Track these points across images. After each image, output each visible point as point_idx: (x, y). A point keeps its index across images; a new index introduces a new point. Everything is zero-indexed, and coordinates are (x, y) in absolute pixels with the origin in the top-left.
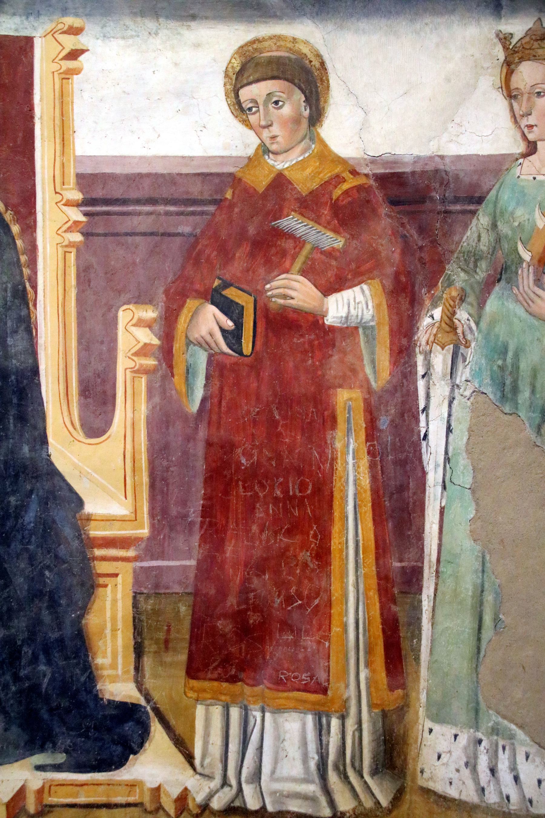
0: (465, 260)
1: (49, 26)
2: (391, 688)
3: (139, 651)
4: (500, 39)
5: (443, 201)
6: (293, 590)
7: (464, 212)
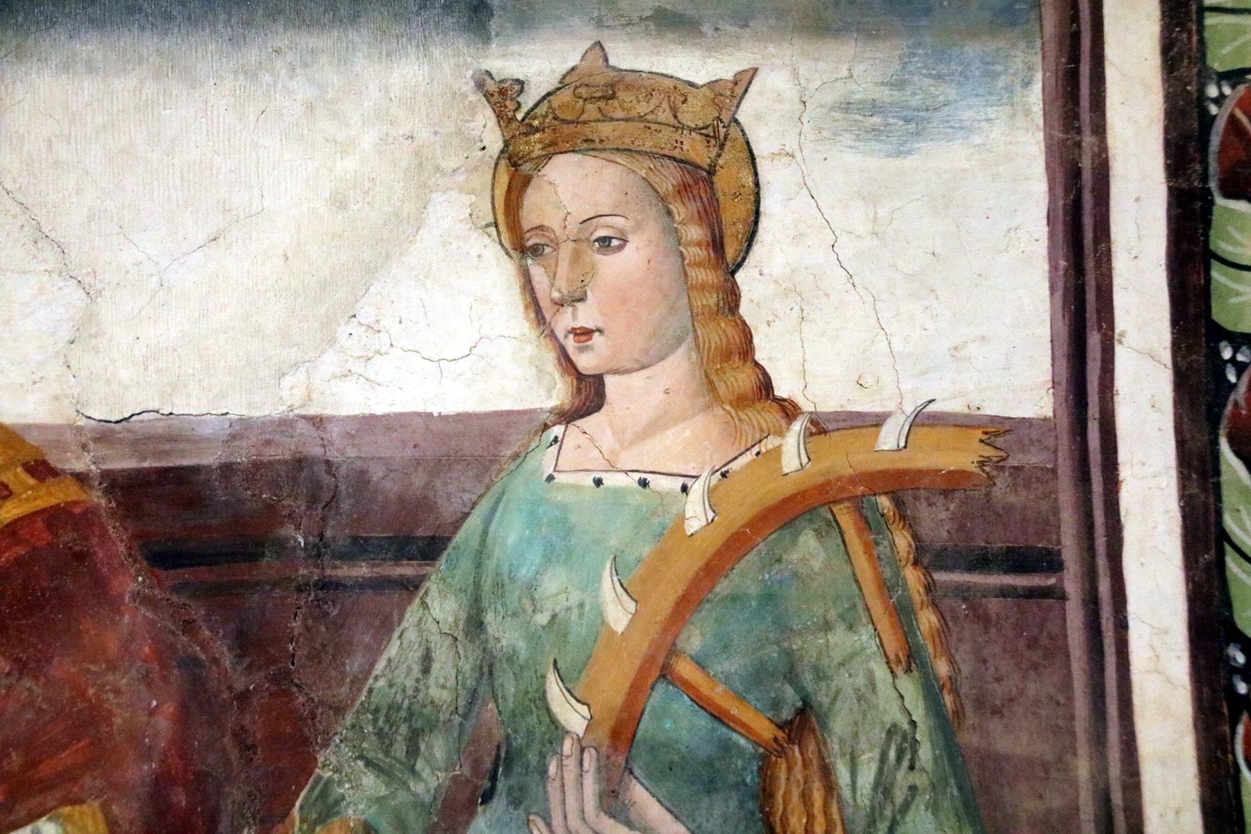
0: (380, 733)
4: (488, 95)
5: (318, 550)
7: (379, 585)
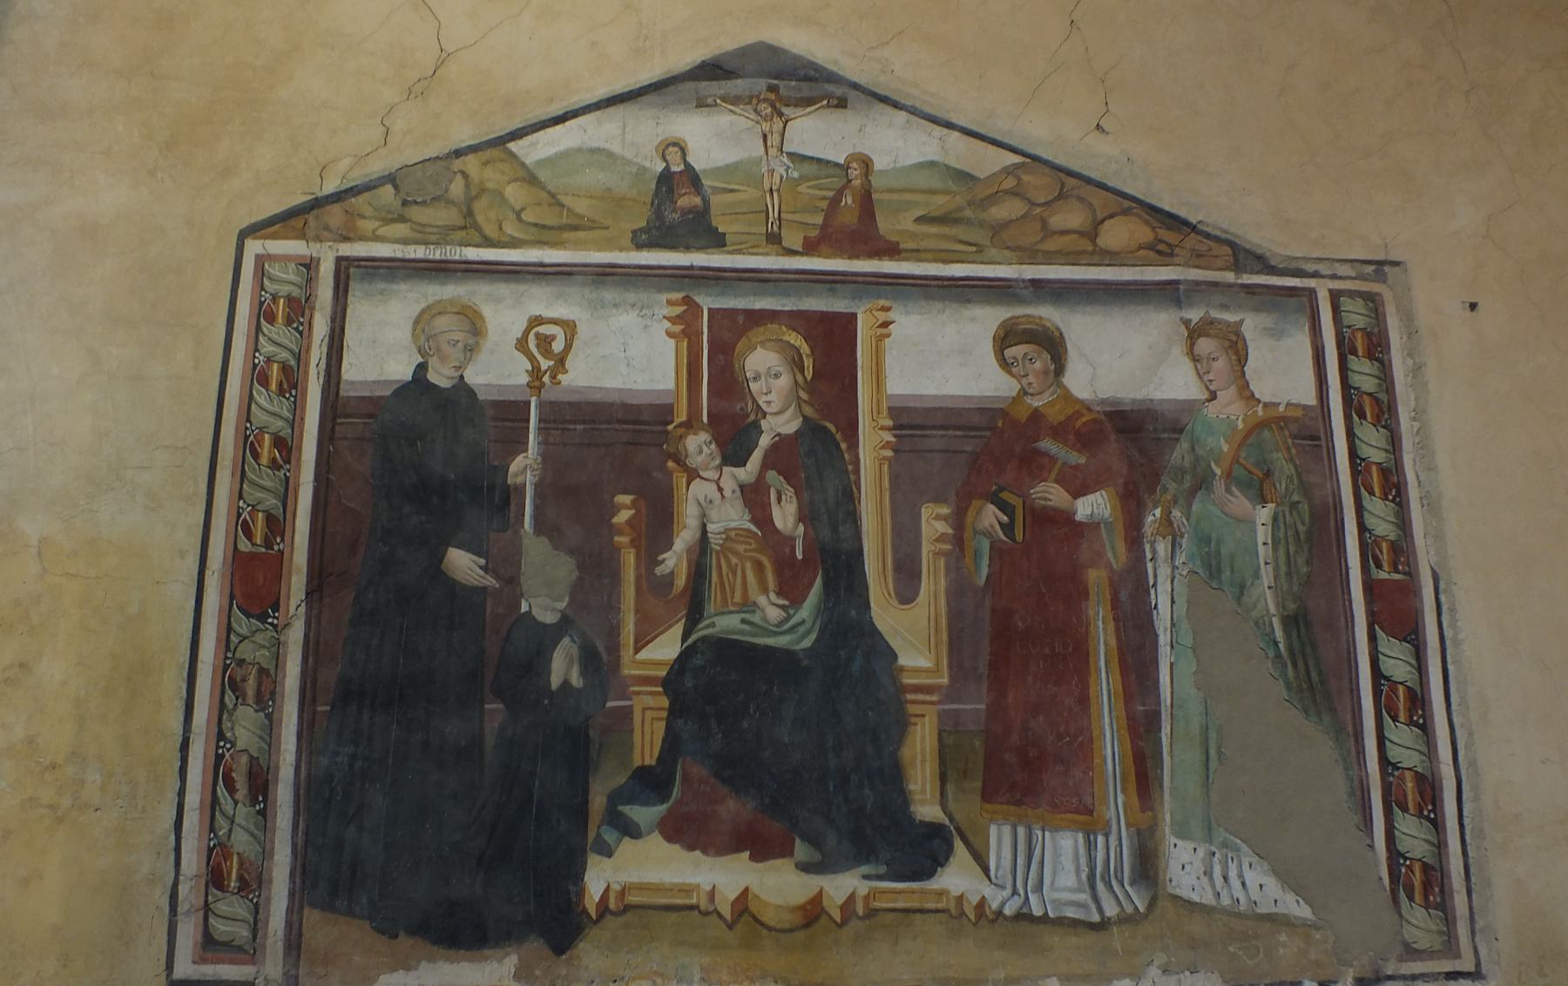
6: (1062, 729)
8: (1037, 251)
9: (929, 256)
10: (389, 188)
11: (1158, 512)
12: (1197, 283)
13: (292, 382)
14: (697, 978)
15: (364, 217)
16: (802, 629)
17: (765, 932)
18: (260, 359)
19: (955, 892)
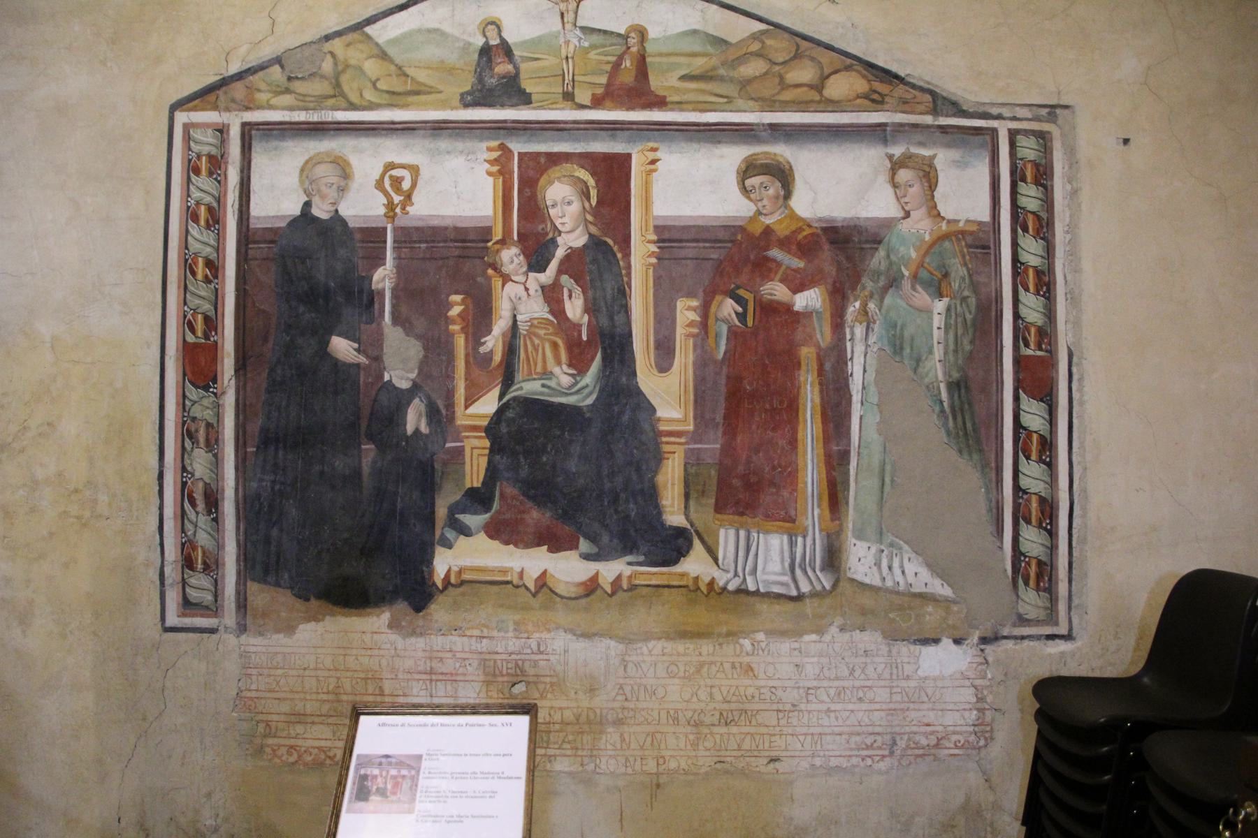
1: (640, 148)
2: (832, 520)
3: (687, 496)
5: (860, 242)
8: (775, 101)
9: (690, 107)
10: (277, 68)
11: (857, 304)
12: (901, 125)
13: (215, 220)
14: (511, 628)
15: (259, 90)
16: (586, 391)
17: (558, 599)
18: (192, 203)
19: (693, 575)
